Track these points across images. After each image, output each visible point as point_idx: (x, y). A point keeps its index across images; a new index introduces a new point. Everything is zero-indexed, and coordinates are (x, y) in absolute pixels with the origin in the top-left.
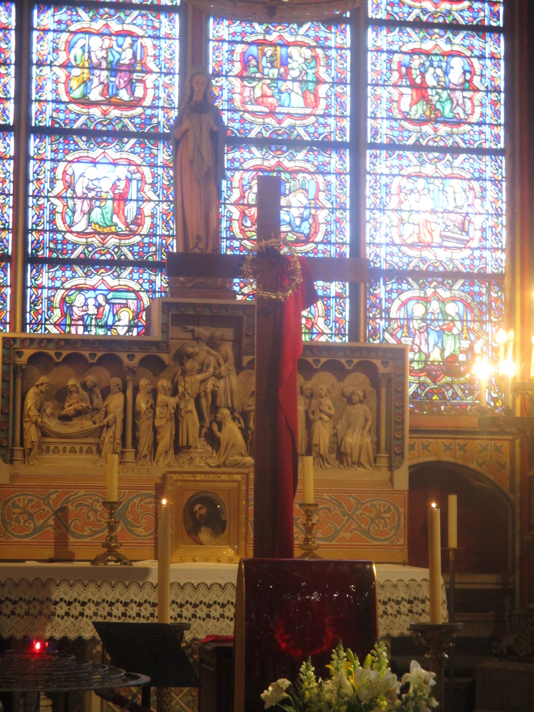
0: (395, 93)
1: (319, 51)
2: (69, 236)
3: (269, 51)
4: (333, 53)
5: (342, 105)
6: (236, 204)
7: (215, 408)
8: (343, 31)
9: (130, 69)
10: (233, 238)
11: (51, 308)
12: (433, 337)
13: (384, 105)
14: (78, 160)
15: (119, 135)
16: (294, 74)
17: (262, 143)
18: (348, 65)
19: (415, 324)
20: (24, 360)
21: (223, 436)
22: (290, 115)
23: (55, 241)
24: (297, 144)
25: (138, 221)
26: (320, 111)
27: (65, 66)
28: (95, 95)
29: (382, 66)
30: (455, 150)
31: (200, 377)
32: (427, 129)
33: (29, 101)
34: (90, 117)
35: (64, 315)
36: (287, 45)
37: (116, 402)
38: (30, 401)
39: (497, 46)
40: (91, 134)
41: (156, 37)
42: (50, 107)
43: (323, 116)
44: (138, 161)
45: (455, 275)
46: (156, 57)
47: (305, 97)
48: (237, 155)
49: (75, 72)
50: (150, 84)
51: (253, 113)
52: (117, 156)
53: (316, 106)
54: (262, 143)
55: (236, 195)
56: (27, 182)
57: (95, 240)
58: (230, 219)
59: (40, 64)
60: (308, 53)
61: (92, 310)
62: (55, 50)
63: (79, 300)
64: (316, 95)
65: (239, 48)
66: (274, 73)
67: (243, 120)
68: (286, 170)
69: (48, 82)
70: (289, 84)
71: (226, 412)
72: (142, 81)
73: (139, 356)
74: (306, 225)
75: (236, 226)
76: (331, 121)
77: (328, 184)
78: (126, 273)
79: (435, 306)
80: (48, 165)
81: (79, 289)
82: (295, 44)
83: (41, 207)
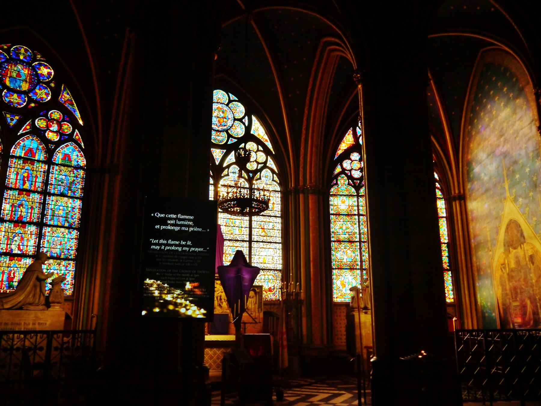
0: (258, 230)
7: (221, 299)
12: (266, 283)
13: (256, 232)
17: (229, 240)
19: (262, 280)
21: (222, 305)
24: (237, 241)
29: (256, 224)
30: (271, 242)
32: (265, 238)
39: (279, 220)
45: (271, 270)
54: (229, 240)
60: (240, 221)
65: (225, 220)
70: (236, 228)
71: (223, 300)
79: (266, 276)
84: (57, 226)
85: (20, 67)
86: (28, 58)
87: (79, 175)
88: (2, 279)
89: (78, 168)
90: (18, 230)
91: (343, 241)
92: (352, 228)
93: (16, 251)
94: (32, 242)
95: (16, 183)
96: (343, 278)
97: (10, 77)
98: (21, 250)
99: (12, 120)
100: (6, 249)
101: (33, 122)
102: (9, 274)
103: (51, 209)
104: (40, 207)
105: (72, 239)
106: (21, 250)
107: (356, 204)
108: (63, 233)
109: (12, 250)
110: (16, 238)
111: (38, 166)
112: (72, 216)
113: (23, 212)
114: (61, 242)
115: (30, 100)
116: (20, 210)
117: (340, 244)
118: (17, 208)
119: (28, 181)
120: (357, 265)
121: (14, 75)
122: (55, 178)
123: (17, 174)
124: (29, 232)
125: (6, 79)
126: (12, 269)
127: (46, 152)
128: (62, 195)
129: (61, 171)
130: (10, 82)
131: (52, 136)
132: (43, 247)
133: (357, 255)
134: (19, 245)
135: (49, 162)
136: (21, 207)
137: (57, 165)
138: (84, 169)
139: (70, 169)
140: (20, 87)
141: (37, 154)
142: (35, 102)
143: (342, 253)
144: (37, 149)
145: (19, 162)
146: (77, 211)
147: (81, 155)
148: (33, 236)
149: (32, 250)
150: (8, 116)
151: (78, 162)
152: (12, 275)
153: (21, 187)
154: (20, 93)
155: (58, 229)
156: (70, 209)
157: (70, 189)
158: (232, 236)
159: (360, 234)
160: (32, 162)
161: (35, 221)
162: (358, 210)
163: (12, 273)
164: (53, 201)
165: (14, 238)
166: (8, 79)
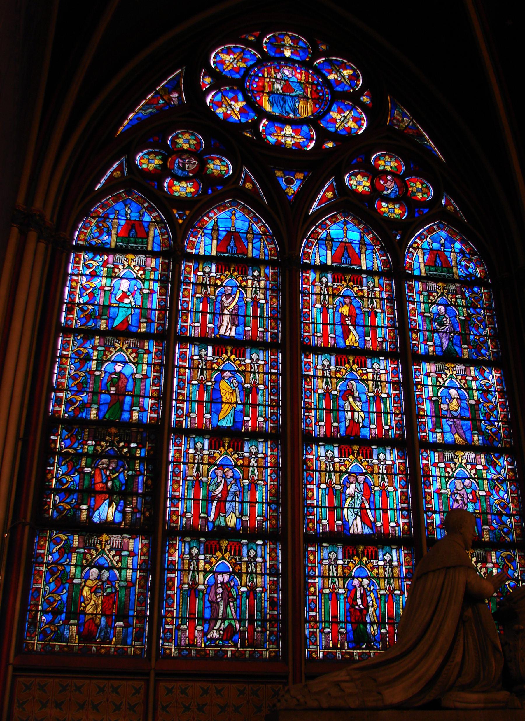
84: (454, 447)
85: (287, 73)
86: (301, 54)
88: (335, 617)
89: (469, 282)
90: (352, 464)
93: (358, 527)
94: (395, 499)
95: (325, 335)
97: (269, 94)
98: (372, 525)
99: (289, 182)
100: (331, 522)
101: (340, 181)
102: (351, 599)
103: (429, 398)
104: (398, 395)
105: (502, 481)
106: (372, 525)
108: (474, 466)
109: (346, 524)
110: (351, 489)
111: (371, 285)
112: (487, 416)
113: (355, 411)
114: (473, 492)
115: (324, 135)
116: (347, 407)
118: (341, 402)
119: (354, 326)
121: (279, 88)
122: (422, 314)
123: (325, 310)
124: (383, 469)
125: (261, 98)
126: (356, 582)
127: (384, 250)
128: (448, 357)
129: (430, 293)
130: (272, 103)
131: (392, 210)
132: (429, 510)
134: (362, 508)
135: (397, 273)
136: (351, 399)
137: (419, 278)
138: (486, 286)
139: (452, 287)
140: (295, 111)
141: (363, 257)
142: (334, 136)
144: (362, 243)
145: (324, 280)
146: (496, 399)
148: (397, 479)
149: (401, 521)
150: (279, 174)
151: (467, 268)
152: (359, 602)
153: (341, 343)
154: (297, 123)
155: (460, 454)
156: (476, 395)
157: (465, 339)
160: (357, 276)
161: (392, 433)
163: (359, 595)
164: (427, 375)
165: (345, 487)
166: (265, 98)
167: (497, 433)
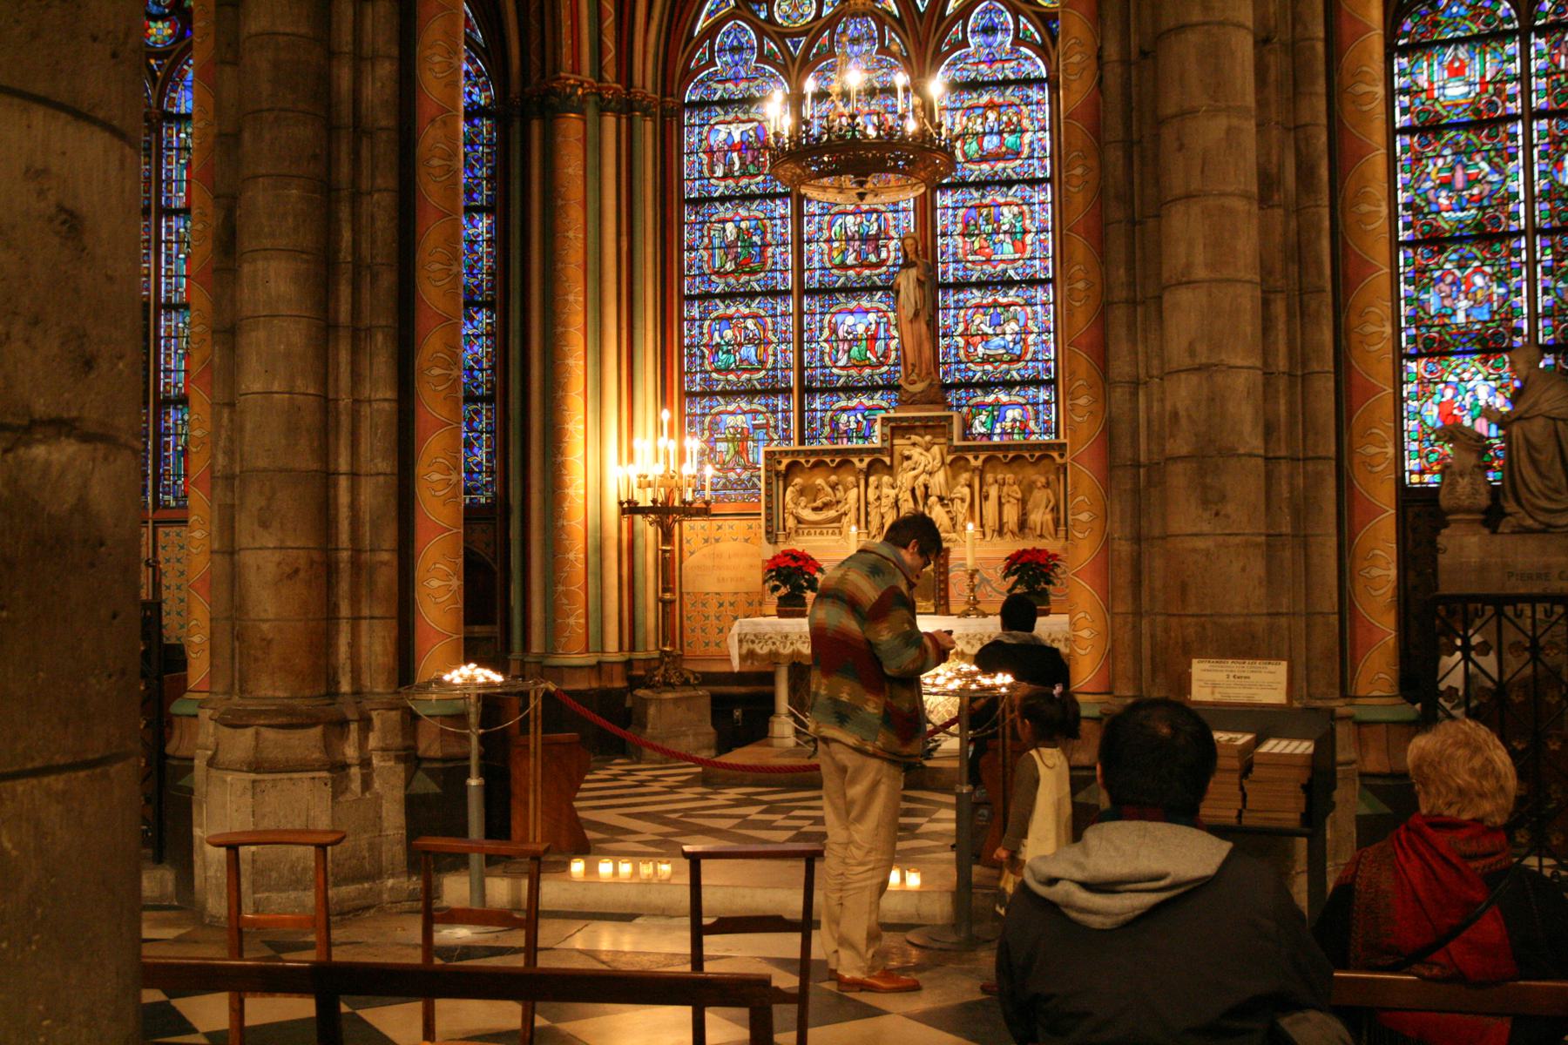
1: (1025, 208)
2: (835, 371)
3: (985, 211)
4: (1037, 207)
5: (1046, 249)
6: (961, 335)
7: (927, 496)
8: (1045, 190)
9: (877, 237)
10: (960, 362)
11: (823, 426)
14: (840, 312)
15: (871, 289)
16: (1006, 227)
18: (1049, 216)
20: (782, 467)
22: (1002, 261)
23: (824, 375)
24: (1010, 283)
25: (886, 355)
26: (1027, 255)
27: (829, 241)
28: (850, 260)
31: (913, 473)
33: (801, 271)
34: (848, 278)
35: (833, 430)
36: (999, 205)
37: (853, 494)
38: (788, 498)
40: (849, 291)
41: (897, 211)
42: (817, 273)
43: (1031, 259)
44: (883, 307)
46: (896, 227)
47: (1013, 244)
48: (961, 296)
49: (836, 244)
50: (892, 247)
51: (973, 262)
52: (868, 305)
53: (1023, 252)
54: (980, 285)
55: (961, 328)
56: (801, 331)
57: (853, 372)
58: (957, 348)
59: (809, 242)
60: (1016, 209)
61: (853, 425)
62: (820, 229)
63: (844, 418)
64: (1023, 243)
65: (961, 212)
66: (989, 228)
67: (965, 269)
68: (1001, 305)
69: (816, 252)
70: (1001, 236)
72: (886, 246)
73: (867, 460)
74: (1018, 347)
75: (962, 352)
76: (1037, 262)
77: (1035, 313)
78: (878, 396)
80: (818, 317)
81: (843, 410)
82: (1006, 204)
83: (814, 350)
87: (477, 135)
91: (1454, 240)
92: (1495, 178)
96: (1449, 393)
105: (477, 337)
107: (1515, 68)
117: (1442, 251)
120: (1518, 331)
133: (1518, 292)
143: (1447, 289)
146: (483, 249)
147: (479, 69)
158: (988, 268)
159: (1531, 200)
162: (1527, 93)
167: (479, 286)
